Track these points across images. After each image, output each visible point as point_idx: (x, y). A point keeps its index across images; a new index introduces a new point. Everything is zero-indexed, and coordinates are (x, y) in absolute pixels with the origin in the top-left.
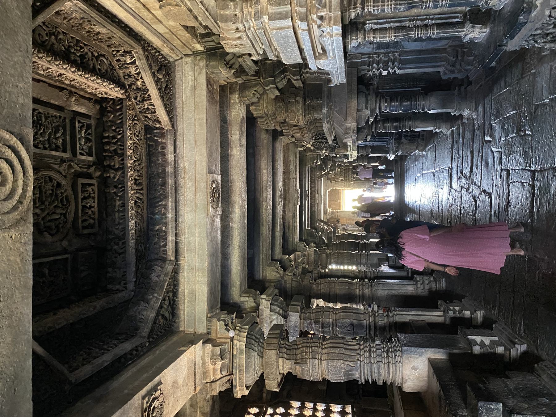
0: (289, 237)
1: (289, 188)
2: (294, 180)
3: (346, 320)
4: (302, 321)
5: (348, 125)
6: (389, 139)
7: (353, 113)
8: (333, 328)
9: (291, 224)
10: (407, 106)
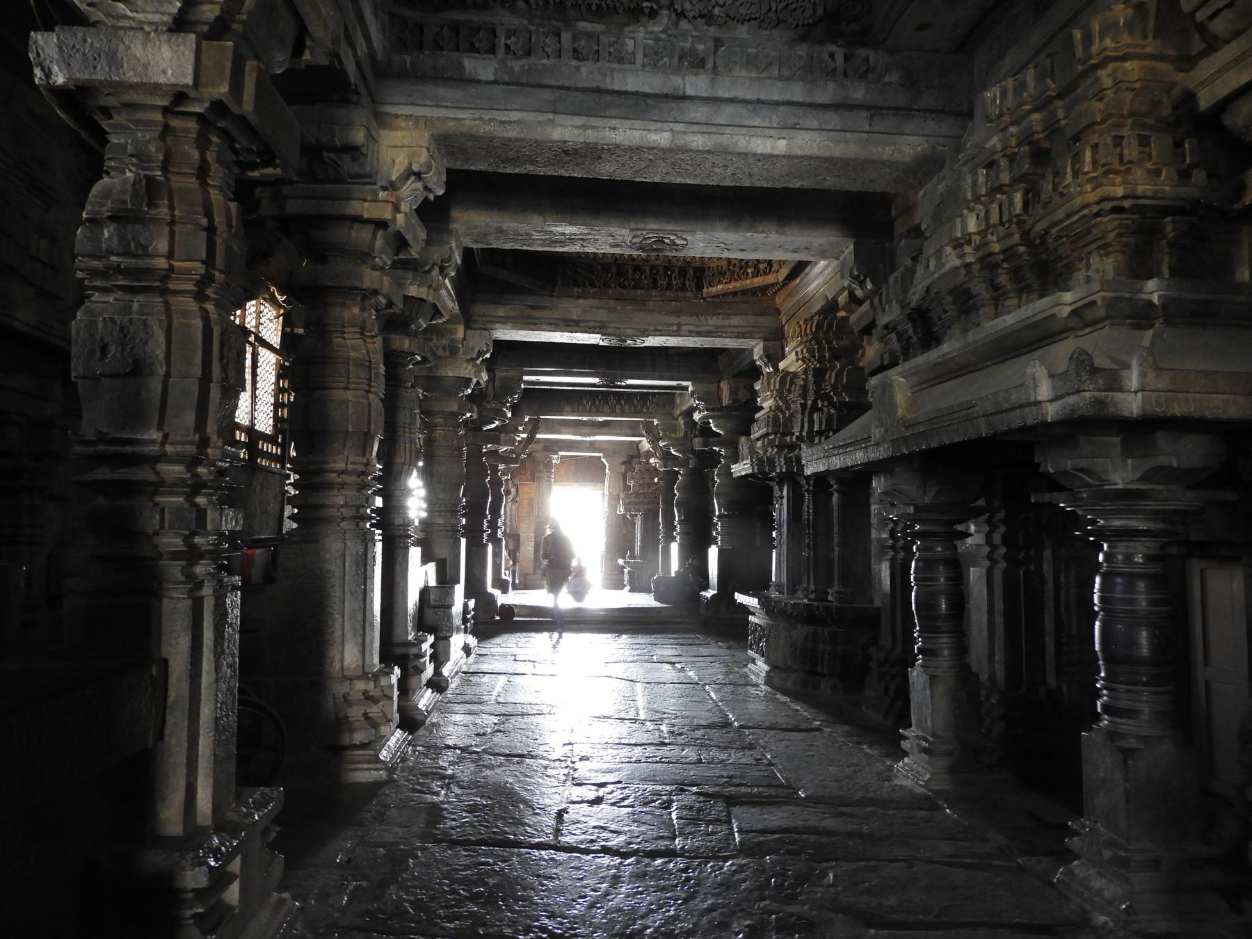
0: (509, 307)
1: (652, 311)
2: (675, 328)
3: (161, 338)
4: (158, 117)
5: (1133, 379)
6: (806, 590)
7: (1187, 401)
8: (118, 270)
9: (546, 314)
10: (1132, 642)
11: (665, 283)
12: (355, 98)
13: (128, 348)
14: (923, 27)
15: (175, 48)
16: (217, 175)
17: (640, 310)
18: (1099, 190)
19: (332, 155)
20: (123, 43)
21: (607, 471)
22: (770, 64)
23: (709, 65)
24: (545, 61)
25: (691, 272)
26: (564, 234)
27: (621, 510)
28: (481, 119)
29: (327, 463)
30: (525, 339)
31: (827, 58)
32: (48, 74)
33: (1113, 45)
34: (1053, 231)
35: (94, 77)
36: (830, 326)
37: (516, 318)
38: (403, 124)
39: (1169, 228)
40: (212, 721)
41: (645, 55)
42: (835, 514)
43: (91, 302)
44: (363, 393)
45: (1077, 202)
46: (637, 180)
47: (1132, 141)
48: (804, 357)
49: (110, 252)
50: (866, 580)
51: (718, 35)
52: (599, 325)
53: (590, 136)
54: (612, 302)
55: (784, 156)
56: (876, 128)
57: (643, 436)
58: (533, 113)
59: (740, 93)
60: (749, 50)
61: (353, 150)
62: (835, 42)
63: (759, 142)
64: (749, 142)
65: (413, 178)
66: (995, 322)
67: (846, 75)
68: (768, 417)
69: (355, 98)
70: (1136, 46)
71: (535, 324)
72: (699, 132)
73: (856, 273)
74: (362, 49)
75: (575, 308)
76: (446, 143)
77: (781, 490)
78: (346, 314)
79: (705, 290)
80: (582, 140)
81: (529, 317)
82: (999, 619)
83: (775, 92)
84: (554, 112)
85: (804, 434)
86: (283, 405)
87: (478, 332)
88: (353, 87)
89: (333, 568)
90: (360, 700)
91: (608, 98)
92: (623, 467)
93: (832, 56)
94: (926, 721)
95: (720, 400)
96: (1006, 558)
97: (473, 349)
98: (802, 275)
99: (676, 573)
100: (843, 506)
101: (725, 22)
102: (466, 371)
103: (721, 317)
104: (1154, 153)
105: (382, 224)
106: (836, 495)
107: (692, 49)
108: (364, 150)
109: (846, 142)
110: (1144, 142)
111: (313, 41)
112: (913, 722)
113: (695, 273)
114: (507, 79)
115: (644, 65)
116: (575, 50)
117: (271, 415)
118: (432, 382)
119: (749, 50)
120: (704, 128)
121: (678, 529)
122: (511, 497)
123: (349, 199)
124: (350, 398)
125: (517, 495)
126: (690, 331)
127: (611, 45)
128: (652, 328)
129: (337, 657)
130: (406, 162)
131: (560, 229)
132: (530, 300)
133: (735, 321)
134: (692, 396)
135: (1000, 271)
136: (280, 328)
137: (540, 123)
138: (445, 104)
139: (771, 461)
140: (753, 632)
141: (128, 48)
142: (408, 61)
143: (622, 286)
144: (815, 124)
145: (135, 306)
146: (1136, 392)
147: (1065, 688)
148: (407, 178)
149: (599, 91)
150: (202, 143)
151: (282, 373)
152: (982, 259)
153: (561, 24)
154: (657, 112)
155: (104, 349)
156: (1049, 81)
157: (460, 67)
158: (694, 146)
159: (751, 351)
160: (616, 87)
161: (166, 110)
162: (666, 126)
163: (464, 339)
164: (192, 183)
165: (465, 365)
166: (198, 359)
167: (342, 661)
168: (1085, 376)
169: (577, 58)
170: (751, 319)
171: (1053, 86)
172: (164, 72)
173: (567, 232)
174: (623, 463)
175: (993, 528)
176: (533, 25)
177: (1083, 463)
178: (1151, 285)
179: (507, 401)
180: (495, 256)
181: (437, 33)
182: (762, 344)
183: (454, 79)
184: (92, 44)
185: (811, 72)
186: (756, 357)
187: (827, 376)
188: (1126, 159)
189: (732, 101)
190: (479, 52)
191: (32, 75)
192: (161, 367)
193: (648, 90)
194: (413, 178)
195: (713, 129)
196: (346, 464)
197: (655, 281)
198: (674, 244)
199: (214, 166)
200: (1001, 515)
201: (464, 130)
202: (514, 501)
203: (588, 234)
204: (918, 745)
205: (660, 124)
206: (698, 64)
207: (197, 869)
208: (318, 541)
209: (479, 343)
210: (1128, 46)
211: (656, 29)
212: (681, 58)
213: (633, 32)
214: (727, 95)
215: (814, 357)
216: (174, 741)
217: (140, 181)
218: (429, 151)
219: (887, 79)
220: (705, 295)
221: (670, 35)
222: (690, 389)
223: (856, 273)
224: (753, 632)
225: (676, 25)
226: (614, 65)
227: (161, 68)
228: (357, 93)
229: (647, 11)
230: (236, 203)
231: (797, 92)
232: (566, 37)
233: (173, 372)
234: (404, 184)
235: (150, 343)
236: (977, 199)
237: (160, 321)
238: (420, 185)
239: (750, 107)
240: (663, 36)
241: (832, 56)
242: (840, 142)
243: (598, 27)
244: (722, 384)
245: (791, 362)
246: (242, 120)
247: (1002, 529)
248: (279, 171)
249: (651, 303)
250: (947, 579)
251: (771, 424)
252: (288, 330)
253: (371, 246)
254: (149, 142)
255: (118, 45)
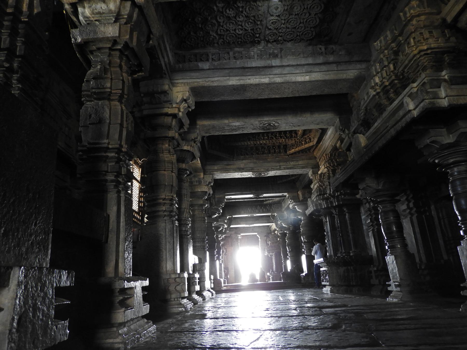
0: (218, 166)
1: (269, 162)
2: (279, 167)
3: (108, 112)
4: (107, 51)
6: (341, 252)
8: (95, 93)
9: (232, 167)
11: (273, 151)
12: (164, 76)
13: (97, 115)
14: (350, 34)
15: (113, 27)
16: (125, 68)
17: (266, 162)
18: (418, 49)
19: (158, 95)
20: (98, 27)
21: (259, 240)
22: (300, 54)
23: (279, 56)
24: (225, 61)
25: (282, 146)
26: (236, 126)
27: (266, 253)
28: (205, 81)
29: (159, 196)
30: (225, 178)
31: (319, 49)
32: (76, 40)
33: (414, 12)
34: (406, 70)
35: (89, 37)
36: (335, 155)
37: (221, 169)
38: (180, 85)
39: (447, 58)
40: (124, 239)
41: (258, 56)
42: (348, 222)
43: (86, 104)
44: (170, 172)
45: (412, 55)
46: (259, 98)
47: (426, 32)
48: (327, 166)
49: (93, 88)
50: (365, 246)
51: (281, 47)
52: (251, 169)
53: (242, 82)
54: (255, 160)
55: (309, 81)
56: (339, 69)
57: (272, 223)
58: (223, 77)
59: (291, 63)
60: (292, 50)
61: (165, 93)
62: (321, 44)
63: (299, 78)
64: (296, 78)
65: (184, 102)
66: (391, 106)
67: (326, 54)
68: (317, 189)
69: (164, 76)
70: (422, 11)
71: (228, 171)
72: (279, 77)
73: (341, 128)
74: (166, 59)
75: (241, 164)
76: (195, 91)
77: (326, 219)
78: (164, 147)
79: (288, 152)
80: (239, 84)
81: (226, 169)
82: (419, 236)
83: (303, 62)
84: (229, 76)
85: (331, 193)
86: (141, 202)
87: (208, 175)
88: (164, 72)
89: (162, 233)
90: (174, 282)
91: (247, 70)
92: (265, 237)
93: (320, 49)
94: (396, 275)
95: (299, 198)
96: (416, 212)
97: (207, 181)
98: (323, 140)
99: (290, 270)
100: (351, 218)
101: (283, 42)
102: (205, 189)
103: (295, 162)
104: (435, 35)
105: (174, 116)
106: (347, 214)
107: (273, 52)
108: (168, 92)
109: (329, 74)
110: (430, 32)
111: (153, 35)
112: (391, 278)
113: (283, 147)
114: (213, 68)
115: (257, 59)
116: (234, 57)
117: (137, 205)
118: (193, 195)
119: (292, 50)
120: (280, 76)
121: (289, 255)
122: (224, 253)
123: (164, 108)
124: (166, 174)
125: (226, 252)
126: (284, 168)
127: (246, 54)
128: (270, 168)
129: (164, 266)
130: (182, 96)
131: (234, 124)
132: (225, 163)
133: (300, 162)
134: (288, 198)
135: (390, 92)
136: (140, 175)
137: (225, 80)
138: (193, 78)
139: (320, 204)
140: (323, 274)
141: (99, 29)
142: (181, 66)
143: (258, 154)
144: (318, 70)
145: (100, 103)
146: (445, 98)
147: (451, 259)
148: (182, 102)
149: (244, 68)
150: (121, 58)
151: (141, 190)
152: (383, 89)
153: (229, 50)
154: (264, 72)
155: (90, 116)
156: (395, 31)
157: (198, 66)
158: (277, 81)
159: (307, 174)
160: (249, 66)
161: (110, 49)
162: (267, 76)
163: (203, 178)
164: (118, 69)
165: (204, 187)
166: (120, 118)
167: (166, 268)
168: (425, 94)
169: (235, 59)
170: (306, 162)
171: (397, 32)
172: (110, 34)
173: (237, 125)
174: (265, 236)
175: (409, 202)
176: (220, 51)
177: (433, 139)
178: (444, 73)
179: (220, 206)
180: (211, 138)
181: (190, 57)
182: (311, 170)
183: (196, 70)
184: (89, 29)
185: (314, 54)
186: (310, 176)
187: (337, 171)
188: (425, 38)
189: (288, 66)
190: (203, 61)
191: (71, 40)
192: (108, 120)
193: (259, 66)
194: (184, 102)
195: (283, 76)
196: (165, 196)
197: (269, 151)
198: (274, 126)
199: (124, 66)
200: (411, 196)
201: (200, 85)
202: (225, 254)
203: (244, 125)
204: (395, 285)
205: (265, 76)
206: (275, 56)
207: (120, 281)
208: (156, 224)
209: (209, 179)
210: (419, 11)
211: (260, 48)
212: (269, 55)
213: (253, 49)
214: (287, 64)
215: (331, 165)
216: (111, 243)
217: (102, 67)
218: (189, 93)
219: (340, 53)
220: (288, 154)
221: (265, 49)
222: (287, 196)
223: (341, 128)
224: (323, 274)
225: (267, 45)
226: (248, 60)
227: (109, 33)
228: (165, 74)
229: (257, 42)
230: (130, 77)
231: (310, 61)
232: (231, 53)
233: (112, 122)
234: (181, 104)
235: (104, 113)
236: (378, 73)
237: (108, 107)
238: (186, 105)
239: (295, 67)
240: (263, 49)
241: (320, 49)
242: (327, 75)
243: (241, 49)
244: (299, 192)
245: (323, 169)
246: (132, 49)
247: (413, 201)
248: (143, 73)
249: (269, 159)
250: (394, 217)
251: (318, 191)
252: (143, 176)
253: (171, 124)
254: (105, 58)
255: (96, 28)
